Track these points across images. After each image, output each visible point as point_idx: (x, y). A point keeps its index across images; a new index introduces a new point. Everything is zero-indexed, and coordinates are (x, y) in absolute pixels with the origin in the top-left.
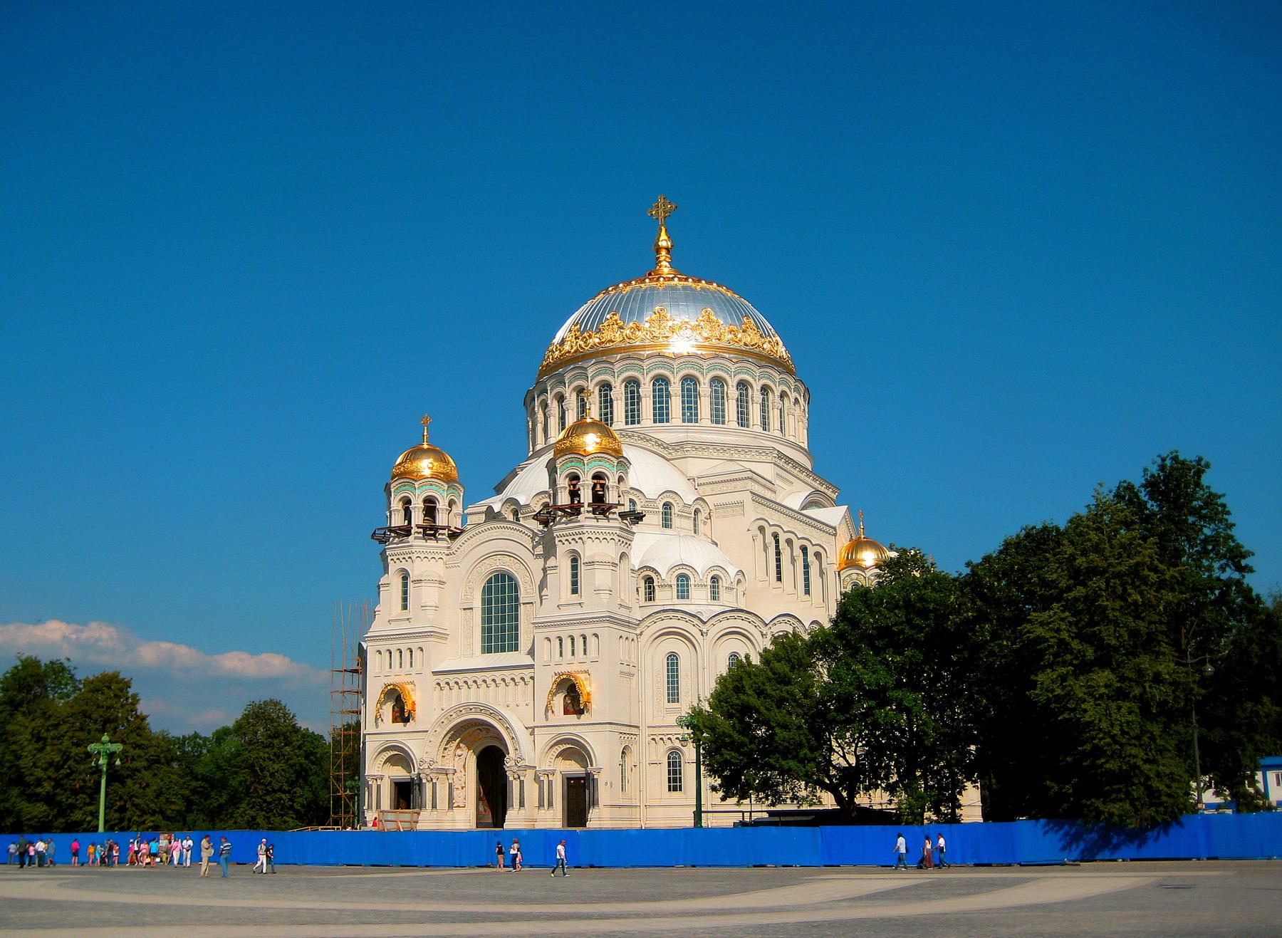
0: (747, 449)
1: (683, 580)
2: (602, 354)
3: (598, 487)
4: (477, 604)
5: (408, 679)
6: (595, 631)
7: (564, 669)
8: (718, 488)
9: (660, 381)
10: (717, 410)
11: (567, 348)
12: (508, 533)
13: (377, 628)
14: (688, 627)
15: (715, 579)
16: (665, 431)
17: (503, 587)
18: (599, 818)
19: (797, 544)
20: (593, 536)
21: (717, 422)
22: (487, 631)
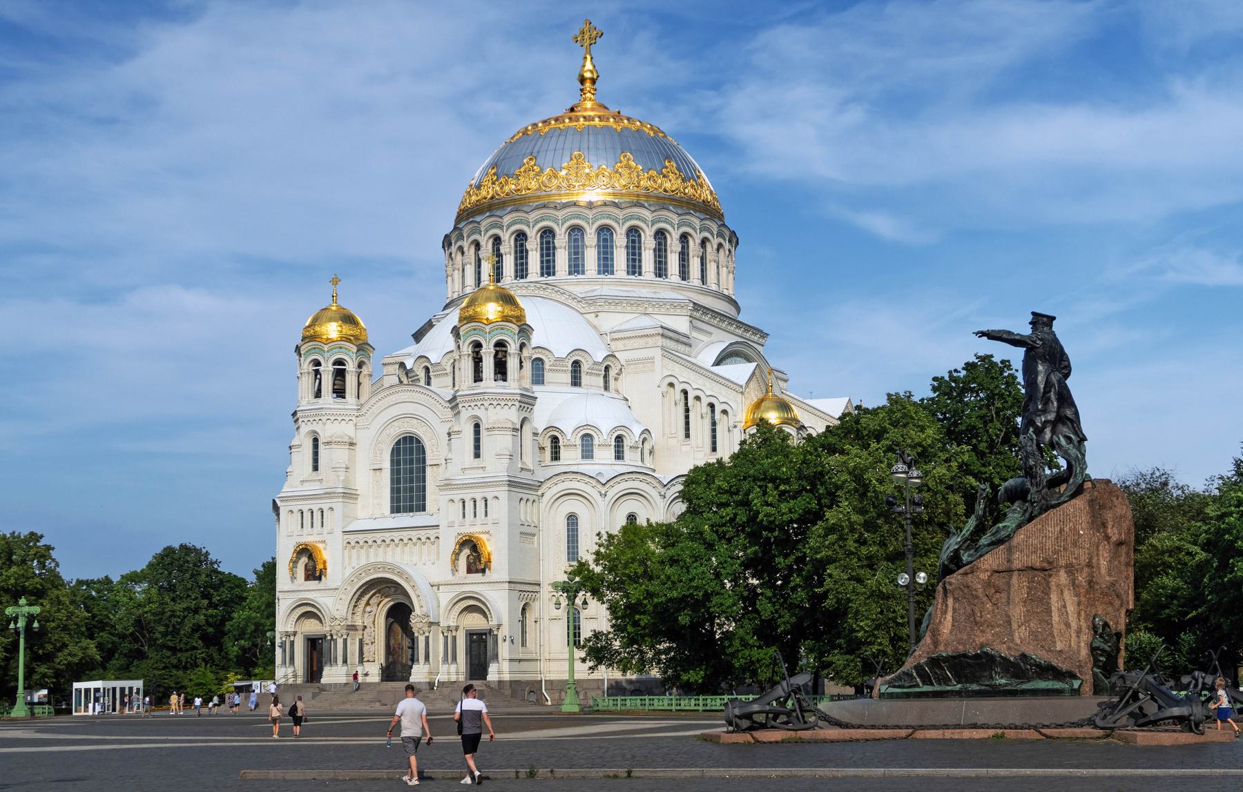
0: (660, 303)
1: (587, 438)
2: (516, 203)
3: (500, 355)
4: (387, 465)
5: (318, 538)
6: (496, 494)
7: (468, 530)
8: (631, 344)
9: (576, 230)
10: (634, 260)
11: (484, 193)
12: (416, 397)
13: (288, 489)
14: (587, 488)
15: (619, 439)
16: (579, 283)
17: (411, 449)
18: (496, 672)
19: (705, 401)
20: (495, 403)
21: (634, 273)
22: (395, 491)
